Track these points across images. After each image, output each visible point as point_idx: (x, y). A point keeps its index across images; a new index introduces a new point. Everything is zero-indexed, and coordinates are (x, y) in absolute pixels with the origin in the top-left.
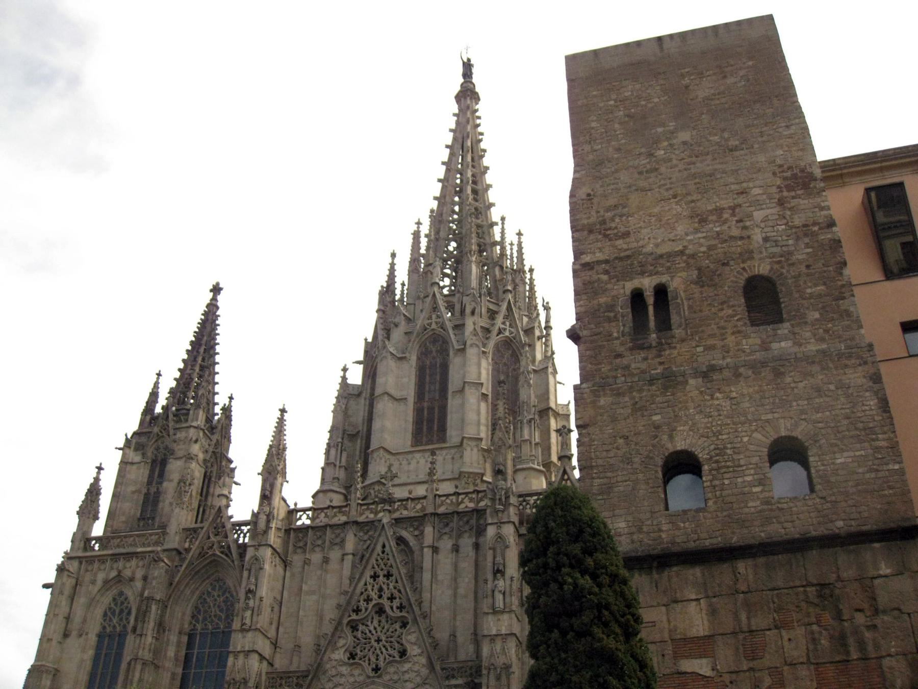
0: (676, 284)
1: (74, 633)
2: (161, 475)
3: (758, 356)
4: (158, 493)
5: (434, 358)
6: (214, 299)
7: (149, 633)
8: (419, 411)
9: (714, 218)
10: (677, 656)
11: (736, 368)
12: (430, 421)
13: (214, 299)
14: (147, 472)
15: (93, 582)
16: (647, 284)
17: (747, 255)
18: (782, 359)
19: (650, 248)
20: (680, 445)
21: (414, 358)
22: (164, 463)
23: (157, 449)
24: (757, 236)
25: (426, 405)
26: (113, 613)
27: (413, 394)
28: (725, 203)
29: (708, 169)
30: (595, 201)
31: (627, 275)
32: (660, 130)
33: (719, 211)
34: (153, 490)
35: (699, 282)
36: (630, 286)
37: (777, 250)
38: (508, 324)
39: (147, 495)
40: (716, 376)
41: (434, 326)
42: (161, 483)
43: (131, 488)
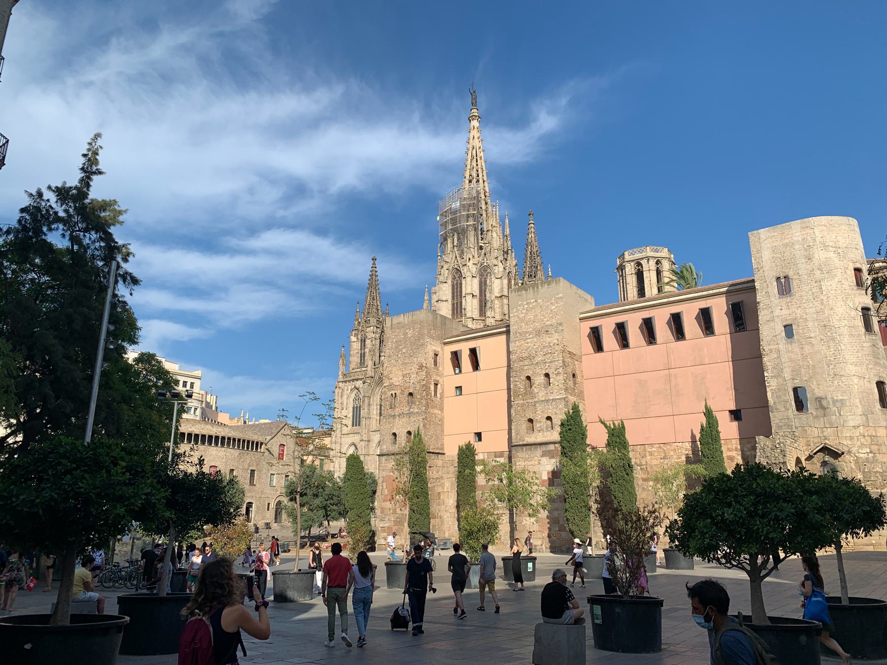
0: (398, 392)
1: (345, 409)
2: (364, 346)
3: (408, 412)
4: (364, 353)
6: (374, 264)
8: (453, 304)
12: (457, 309)
13: (374, 264)
15: (347, 390)
16: (393, 392)
17: (409, 387)
18: (412, 412)
19: (394, 383)
21: (450, 281)
22: (365, 341)
24: (411, 383)
25: (455, 302)
28: (408, 372)
31: (390, 390)
34: (363, 352)
35: (401, 393)
36: (391, 393)
38: (485, 259)
39: (361, 354)
41: (456, 266)
42: (364, 349)
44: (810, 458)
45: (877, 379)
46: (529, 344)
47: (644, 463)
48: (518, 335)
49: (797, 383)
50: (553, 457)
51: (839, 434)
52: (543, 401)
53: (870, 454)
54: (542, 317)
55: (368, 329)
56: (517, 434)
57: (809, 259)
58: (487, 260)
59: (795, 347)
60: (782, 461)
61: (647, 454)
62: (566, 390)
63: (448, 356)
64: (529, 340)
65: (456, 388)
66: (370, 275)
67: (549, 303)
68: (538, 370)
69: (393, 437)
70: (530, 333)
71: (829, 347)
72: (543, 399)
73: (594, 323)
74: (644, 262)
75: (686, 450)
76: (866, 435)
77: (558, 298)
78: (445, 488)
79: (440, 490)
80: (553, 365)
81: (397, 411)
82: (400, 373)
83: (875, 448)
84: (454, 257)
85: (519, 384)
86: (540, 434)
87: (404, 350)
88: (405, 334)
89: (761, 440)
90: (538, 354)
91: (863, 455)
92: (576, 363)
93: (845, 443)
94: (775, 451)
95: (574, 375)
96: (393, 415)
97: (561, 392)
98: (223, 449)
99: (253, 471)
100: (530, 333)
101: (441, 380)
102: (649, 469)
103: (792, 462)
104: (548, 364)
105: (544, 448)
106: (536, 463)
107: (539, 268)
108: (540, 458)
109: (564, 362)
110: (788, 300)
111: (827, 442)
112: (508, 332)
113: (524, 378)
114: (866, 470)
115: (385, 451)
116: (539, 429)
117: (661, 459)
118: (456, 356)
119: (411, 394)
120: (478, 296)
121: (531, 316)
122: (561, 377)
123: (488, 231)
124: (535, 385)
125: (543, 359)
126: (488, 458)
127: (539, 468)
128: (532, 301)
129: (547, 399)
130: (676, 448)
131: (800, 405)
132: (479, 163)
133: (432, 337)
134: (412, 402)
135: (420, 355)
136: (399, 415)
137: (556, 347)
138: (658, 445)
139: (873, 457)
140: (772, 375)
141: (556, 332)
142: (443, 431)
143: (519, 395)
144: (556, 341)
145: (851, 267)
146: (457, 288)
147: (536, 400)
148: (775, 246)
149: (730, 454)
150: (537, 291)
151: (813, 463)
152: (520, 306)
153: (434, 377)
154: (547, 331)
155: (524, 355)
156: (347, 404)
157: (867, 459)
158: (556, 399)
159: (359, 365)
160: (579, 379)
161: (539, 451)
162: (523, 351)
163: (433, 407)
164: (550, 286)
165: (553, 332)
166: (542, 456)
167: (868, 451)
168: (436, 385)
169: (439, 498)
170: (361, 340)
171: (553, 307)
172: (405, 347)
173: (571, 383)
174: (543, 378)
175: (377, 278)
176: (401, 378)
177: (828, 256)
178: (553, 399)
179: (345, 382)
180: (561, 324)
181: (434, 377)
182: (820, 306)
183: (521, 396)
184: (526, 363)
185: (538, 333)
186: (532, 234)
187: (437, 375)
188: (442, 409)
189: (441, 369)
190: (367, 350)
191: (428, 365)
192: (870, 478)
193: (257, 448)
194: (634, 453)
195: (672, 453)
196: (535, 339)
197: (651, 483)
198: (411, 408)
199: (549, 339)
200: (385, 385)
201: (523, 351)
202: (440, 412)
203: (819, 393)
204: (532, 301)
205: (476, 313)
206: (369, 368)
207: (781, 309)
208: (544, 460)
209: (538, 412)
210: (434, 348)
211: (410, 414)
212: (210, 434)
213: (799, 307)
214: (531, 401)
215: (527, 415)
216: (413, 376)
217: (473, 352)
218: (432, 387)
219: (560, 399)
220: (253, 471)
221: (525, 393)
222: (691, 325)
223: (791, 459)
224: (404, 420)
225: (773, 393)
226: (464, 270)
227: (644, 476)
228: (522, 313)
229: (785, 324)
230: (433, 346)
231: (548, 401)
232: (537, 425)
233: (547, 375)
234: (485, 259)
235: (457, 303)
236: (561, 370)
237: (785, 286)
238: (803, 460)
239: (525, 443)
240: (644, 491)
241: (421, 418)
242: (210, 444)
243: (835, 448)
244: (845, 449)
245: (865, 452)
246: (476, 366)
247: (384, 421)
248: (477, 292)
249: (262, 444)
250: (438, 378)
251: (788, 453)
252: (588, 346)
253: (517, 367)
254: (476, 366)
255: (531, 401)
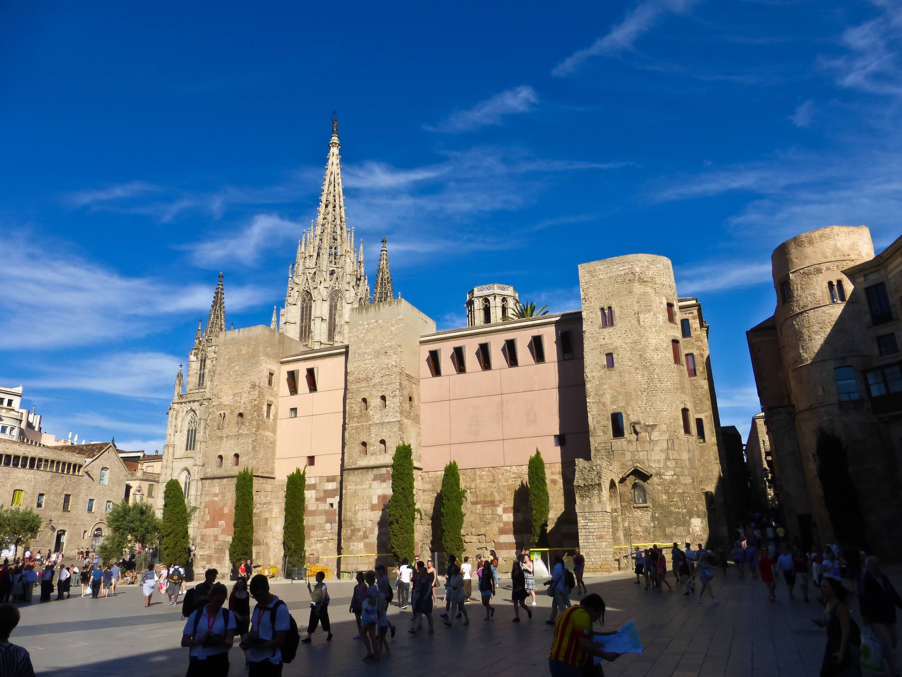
1: (179, 431)
2: (204, 366)
5: (307, 303)
7: (202, 432)
8: (301, 327)
9: (358, 282)
10: (214, 497)
11: (232, 435)
12: (305, 332)
14: (199, 365)
16: (222, 412)
17: (239, 407)
18: (240, 435)
19: (224, 403)
20: (220, 454)
21: (300, 303)
22: (205, 361)
23: (202, 355)
26: (192, 422)
27: (299, 320)
29: (238, 380)
30: (218, 386)
32: (233, 364)
33: (237, 393)
34: (202, 372)
36: (219, 413)
37: (245, 406)
38: (337, 283)
39: (200, 374)
40: (229, 438)
41: (306, 289)
42: (204, 369)
43: (195, 372)
44: (622, 480)
45: (682, 406)
46: (367, 366)
47: (473, 486)
48: (357, 355)
49: (614, 408)
50: (384, 481)
51: (649, 457)
52: (377, 424)
53: (674, 477)
54: (382, 338)
55: (209, 349)
56: (350, 458)
57: (629, 293)
58: (339, 284)
59: (614, 374)
60: (597, 482)
61: (477, 478)
62: (401, 412)
63: (285, 376)
64: (367, 361)
65: (291, 409)
66: (215, 293)
67: (390, 324)
68: (374, 393)
69: (219, 460)
70: (369, 354)
71: (643, 375)
72: (378, 422)
73: (433, 347)
74: (491, 299)
75: (514, 474)
76: (672, 458)
77: (399, 319)
78: (274, 513)
79: (267, 515)
80: (390, 387)
81: (226, 432)
82: (231, 392)
83: (678, 470)
84: (305, 280)
85: (355, 406)
86: (373, 457)
87: (237, 368)
88: (239, 351)
89: (580, 463)
90: (375, 375)
91: (668, 477)
92: (414, 386)
93: (654, 466)
94: (592, 473)
95: (410, 399)
96: (221, 437)
97: (396, 415)
98: (32, 471)
99: (67, 497)
100: (369, 354)
101: (275, 401)
102: (478, 493)
103: (606, 484)
104: (385, 387)
105: (376, 471)
106: (368, 487)
107: (389, 294)
108: (372, 482)
109: (401, 384)
110: (610, 331)
111: (638, 465)
112: (346, 354)
113: (360, 400)
114: (670, 491)
115: (209, 475)
116: (373, 452)
117: (490, 482)
118: (292, 378)
119: (241, 415)
120: (328, 320)
121: (370, 337)
122: (397, 400)
123: (342, 255)
124: (370, 408)
125: (381, 381)
126: (320, 483)
127: (370, 493)
128: (372, 321)
129: (382, 421)
130: (504, 471)
131: (618, 431)
132: (336, 189)
133: (267, 355)
134: (242, 423)
135: (253, 373)
136: (227, 437)
137: (394, 369)
138: (487, 469)
139: (677, 479)
140: (593, 401)
141: (394, 354)
142: (274, 454)
143: (354, 418)
144: (394, 363)
145: (665, 302)
146: (306, 311)
147: (371, 422)
148: (601, 279)
149: (553, 477)
150: (379, 311)
151: (626, 485)
152: (360, 325)
153: (268, 398)
154: (386, 353)
155: (361, 376)
156: (181, 427)
157: (671, 480)
158: (391, 422)
159: (197, 385)
160: (415, 402)
161: (371, 474)
162: (361, 372)
163: (265, 429)
164: (391, 307)
165: (392, 354)
166: (373, 480)
167: (673, 473)
168: (269, 406)
169: (266, 524)
170: (201, 360)
171: (393, 329)
172: (237, 364)
173: (407, 406)
174: (379, 400)
175: (223, 296)
176: (231, 398)
177: (646, 291)
178: (388, 422)
179: (181, 403)
180: (400, 346)
181: (268, 398)
182: (636, 337)
183: (355, 419)
184: (363, 385)
185: (377, 354)
186: (384, 260)
187: (271, 395)
188: (274, 431)
189: (275, 389)
190: (206, 371)
191: (262, 384)
192: (674, 498)
193: (74, 471)
194: (464, 477)
195: (500, 476)
196: (374, 360)
197: (479, 506)
198: (240, 429)
199: (387, 360)
200: (213, 404)
201: (361, 372)
202: (272, 434)
203: (633, 418)
204: (372, 321)
205: (324, 337)
206: (207, 390)
207: (604, 339)
208: (376, 484)
209: (372, 435)
210: (270, 367)
211: (238, 436)
212: (16, 454)
213: (620, 337)
214: (366, 424)
215: (361, 438)
216: (244, 395)
217: (311, 373)
218: (265, 408)
219: (394, 422)
220: (67, 497)
221: (360, 416)
222: (523, 353)
223: (606, 481)
224: (232, 442)
225: (593, 418)
226: (314, 294)
227: (474, 500)
228: (362, 333)
229: (607, 352)
230: (268, 365)
231: (382, 424)
232: (370, 449)
233: (383, 398)
234: (337, 283)
235: (306, 327)
236: (397, 393)
237: (608, 318)
238: (617, 481)
239: (357, 466)
240: (472, 514)
241: (250, 440)
242: (24, 466)
243: (644, 470)
244: (653, 472)
245: (670, 474)
246: (313, 387)
247: (210, 442)
248: (326, 316)
249: (80, 466)
250: (271, 399)
251: (603, 475)
252: (426, 370)
253: (353, 388)
254: (313, 387)
255: (366, 424)
